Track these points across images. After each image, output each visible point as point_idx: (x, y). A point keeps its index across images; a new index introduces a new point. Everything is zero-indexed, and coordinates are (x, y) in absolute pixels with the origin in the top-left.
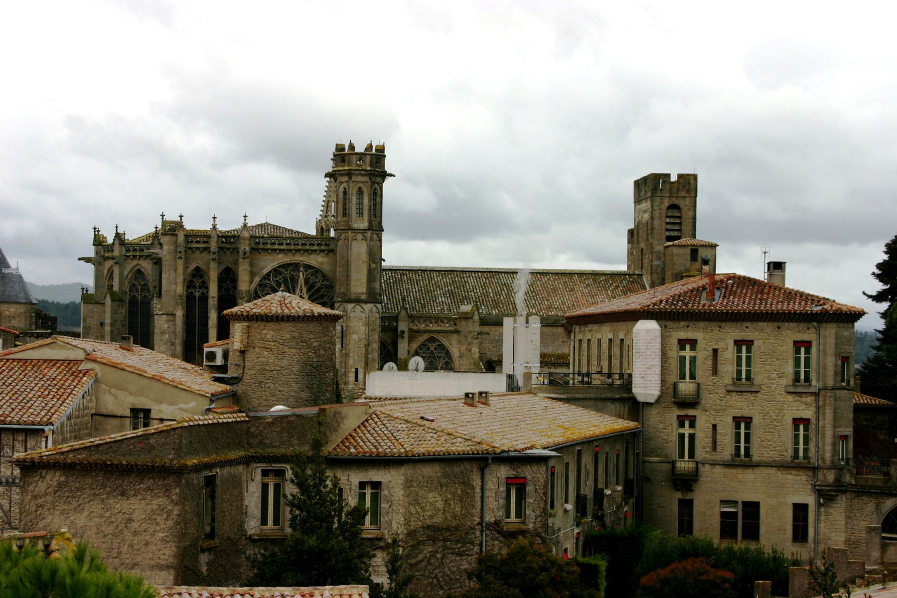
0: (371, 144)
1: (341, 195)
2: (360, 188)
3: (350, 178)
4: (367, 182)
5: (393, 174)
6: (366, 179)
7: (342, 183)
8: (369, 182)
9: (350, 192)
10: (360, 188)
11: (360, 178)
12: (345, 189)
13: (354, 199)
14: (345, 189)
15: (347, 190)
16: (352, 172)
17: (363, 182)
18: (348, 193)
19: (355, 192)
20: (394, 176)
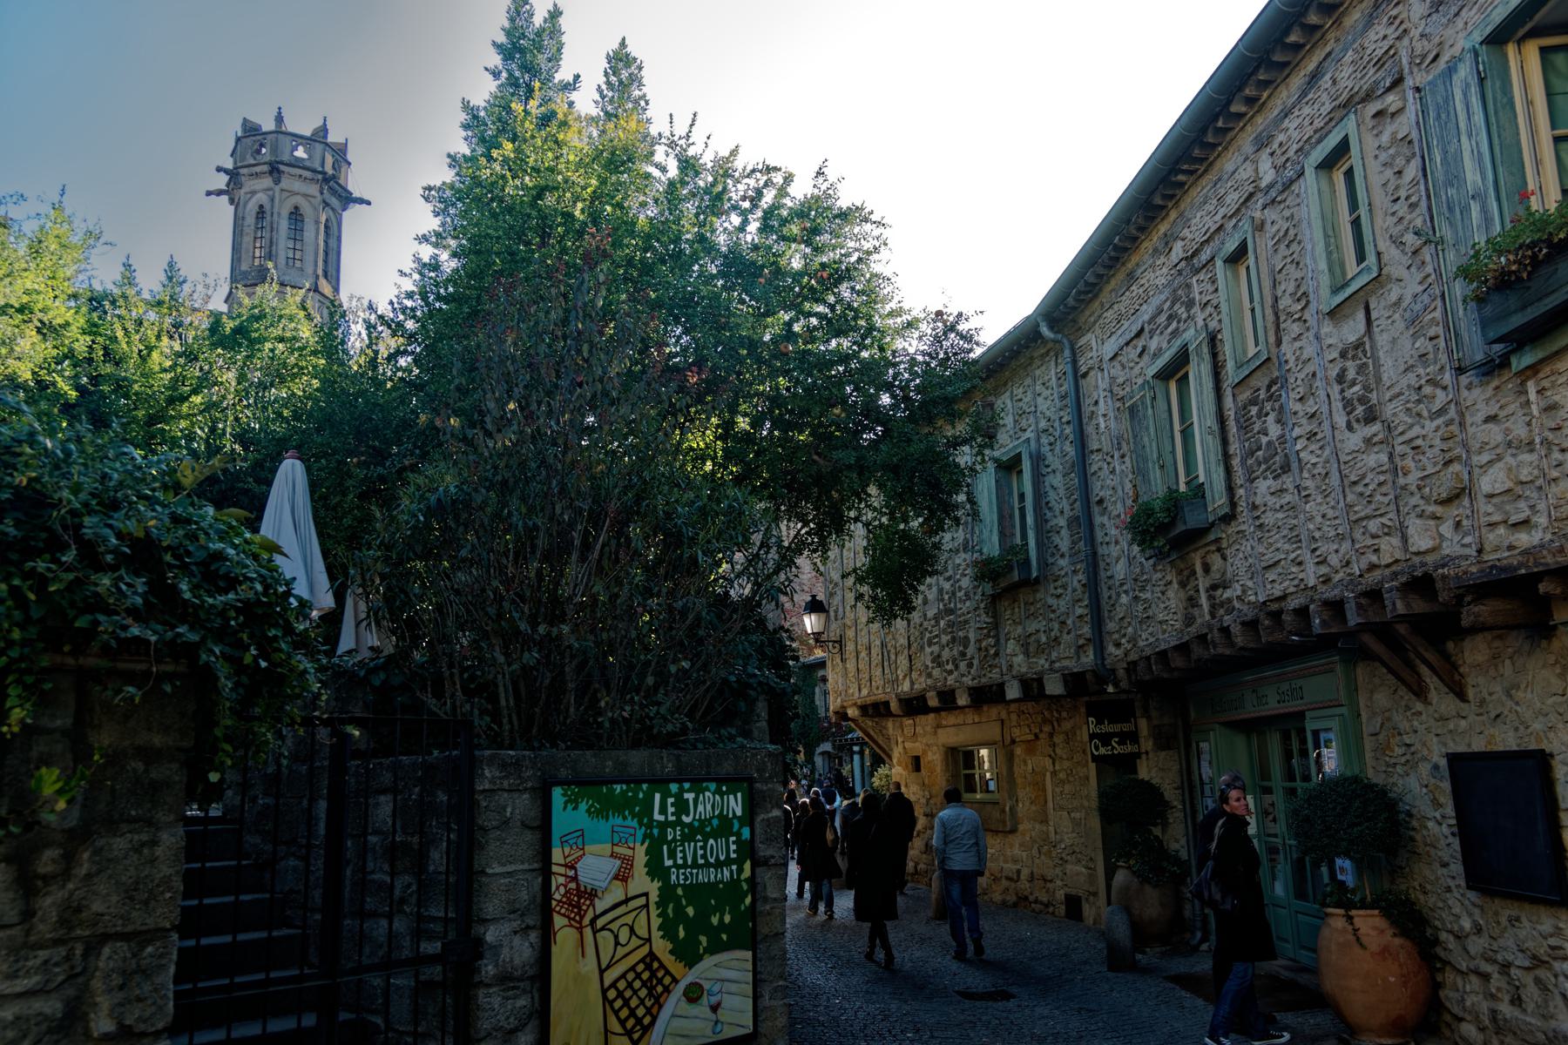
0: (325, 124)
1: (250, 220)
2: (296, 208)
3: (278, 182)
4: (314, 197)
5: (366, 197)
6: (313, 189)
7: (253, 193)
8: (319, 198)
9: (276, 210)
10: (296, 208)
11: (297, 186)
12: (261, 207)
13: (284, 225)
14: (261, 207)
15: (267, 207)
16: (282, 167)
17: (306, 196)
18: (269, 213)
19: (285, 213)
20: (369, 203)
